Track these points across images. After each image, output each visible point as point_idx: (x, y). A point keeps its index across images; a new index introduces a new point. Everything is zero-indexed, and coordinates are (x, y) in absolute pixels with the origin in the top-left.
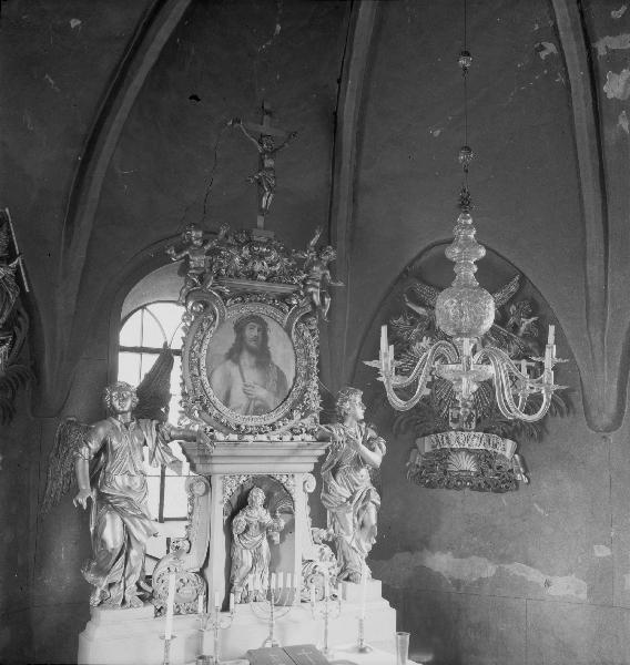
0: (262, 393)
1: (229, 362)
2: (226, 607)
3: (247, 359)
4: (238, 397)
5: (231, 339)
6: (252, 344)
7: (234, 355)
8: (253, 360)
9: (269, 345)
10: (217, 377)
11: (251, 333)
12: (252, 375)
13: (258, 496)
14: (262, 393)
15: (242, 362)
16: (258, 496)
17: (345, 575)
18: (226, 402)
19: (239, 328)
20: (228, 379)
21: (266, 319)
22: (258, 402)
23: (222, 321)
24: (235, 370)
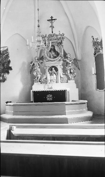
0: (55, 55)
1: (50, 52)
2: (50, 83)
3: (52, 51)
4: (52, 57)
7: (50, 51)
8: (53, 51)
10: (48, 55)
12: (53, 53)
13: (53, 69)
14: (55, 55)
16: (53, 69)
17: (69, 79)
18: (50, 57)
21: (54, 45)
24: (51, 53)
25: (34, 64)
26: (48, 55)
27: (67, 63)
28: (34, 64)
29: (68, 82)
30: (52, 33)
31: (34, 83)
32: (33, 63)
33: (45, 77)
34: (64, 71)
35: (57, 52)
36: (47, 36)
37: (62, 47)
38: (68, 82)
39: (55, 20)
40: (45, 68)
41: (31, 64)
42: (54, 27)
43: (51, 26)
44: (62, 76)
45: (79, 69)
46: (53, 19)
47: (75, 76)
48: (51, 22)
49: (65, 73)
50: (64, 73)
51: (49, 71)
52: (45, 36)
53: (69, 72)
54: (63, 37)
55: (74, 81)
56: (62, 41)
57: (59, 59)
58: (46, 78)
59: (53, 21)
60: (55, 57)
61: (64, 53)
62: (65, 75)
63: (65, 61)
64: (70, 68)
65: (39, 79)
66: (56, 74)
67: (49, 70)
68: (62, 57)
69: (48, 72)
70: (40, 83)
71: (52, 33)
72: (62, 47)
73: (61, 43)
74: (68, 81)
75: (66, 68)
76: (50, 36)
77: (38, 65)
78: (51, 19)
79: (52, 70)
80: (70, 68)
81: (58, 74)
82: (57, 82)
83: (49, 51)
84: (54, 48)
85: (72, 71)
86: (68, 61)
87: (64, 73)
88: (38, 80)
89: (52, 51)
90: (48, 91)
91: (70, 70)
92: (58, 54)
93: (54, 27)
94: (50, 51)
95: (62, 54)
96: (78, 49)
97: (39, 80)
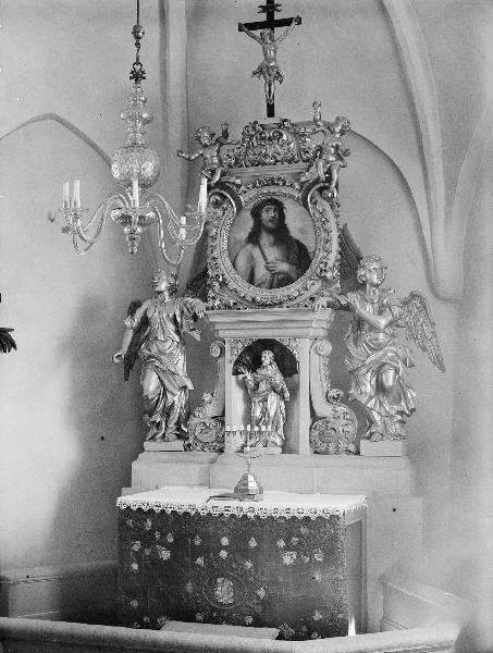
0: (284, 267)
1: (250, 245)
3: (265, 239)
4: (261, 273)
5: (248, 223)
6: (270, 225)
7: (254, 238)
8: (272, 239)
9: (287, 222)
10: (242, 262)
11: (268, 215)
12: (273, 253)
14: (284, 267)
15: (262, 243)
16: (267, 357)
18: (251, 280)
19: (256, 213)
20: (251, 258)
22: (280, 277)
23: (240, 207)
24: (256, 252)
25: (145, 321)
26: (242, 262)
27: (360, 323)
28: (145, 321)
29: (358, 453)
30: (271, 113)
31: (147, 445)
32: (144, 307)
33: (211, 410)
34: (341, 378)
35: (298, 241)
36: (236, 134)
37: (330, 214)
38: (358, 453)
39: (287, 22)
40: (215, 352)
41: (128, 323)
42: (279, 76)
43: (260, 71)
44: (323, 409)
45: (439, 362)
46: (278, 16)
47: (413, 410)
48: (262, 40)
49: (345, 387)
50: (334, 393)
51: (236, 373)
52: (219, 134)
53: (368, 387)
54: (337, 148)
55: (398, 447)
56: (329, 172)
57: (308, 294)
58: (220, 418)
59: (278, 31)
60: (286, 280)
61: (340, 244)
62: (345, 400)
63: (347, 308)
64: (373, 357)
65: (174, 418)
66: (281, 394)
67: (237, 362)
68: (324, 279)
69: (231, 382)
70: (180, 444)
71: (271, 113)
72: (330, 214)
73: (327, 188)
74: (364, 444)
75: (350, 356)
76: (256, 133)
77: (171, 327)
78: (263, 17)
79: (256, 364)
80: (373, 357)
81: (294, 390)
82: (292, 442)
83: (244, 234)
84: (282, 216)
85: (389, 379)
86: (367, 311)
87: (334, 393)
88: (172, 425)
89: (265, 239)
90: (216, 513)
91: (379, 371)
92: (300, 258)
93: (283, 73)
94: (250, 234)
95: (330, 264)
96: (448, 214)
97: (179, 429)
